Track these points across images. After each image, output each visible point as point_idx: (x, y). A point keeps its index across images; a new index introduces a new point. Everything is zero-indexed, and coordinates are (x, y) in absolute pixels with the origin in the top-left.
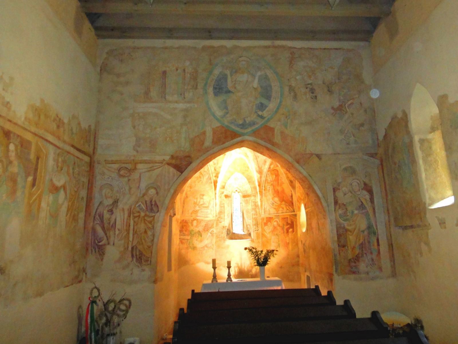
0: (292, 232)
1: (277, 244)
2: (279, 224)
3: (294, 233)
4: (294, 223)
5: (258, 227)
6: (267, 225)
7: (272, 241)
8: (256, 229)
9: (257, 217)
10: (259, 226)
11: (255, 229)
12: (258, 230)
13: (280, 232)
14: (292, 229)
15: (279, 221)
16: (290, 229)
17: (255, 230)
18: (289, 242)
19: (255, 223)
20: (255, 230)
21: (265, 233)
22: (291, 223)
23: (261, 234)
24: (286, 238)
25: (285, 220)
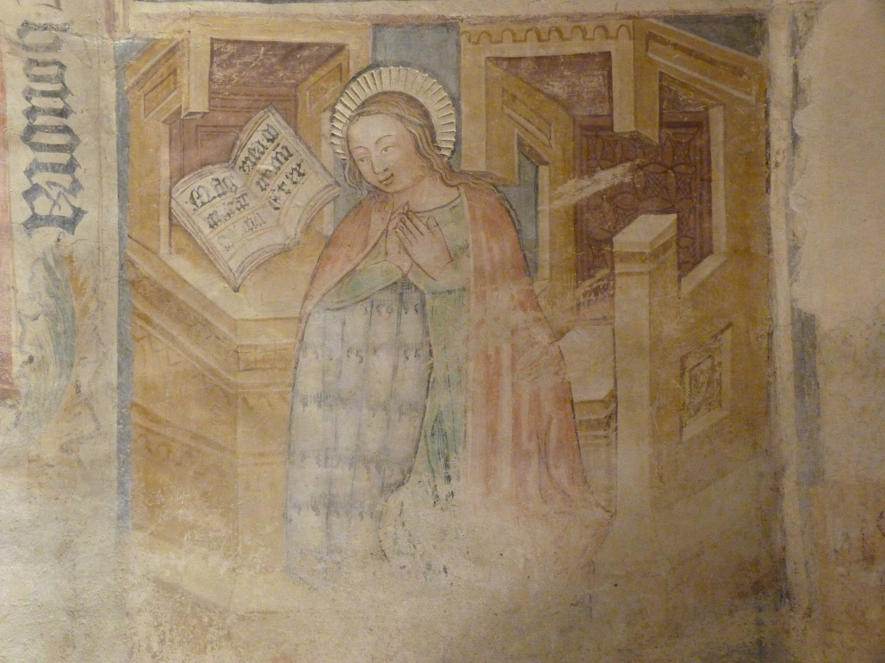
0: (671, 256)
1: (405, 428)
2: (445, 140)
3: (707, 267)
4: (717, 131)
5: (70, 167)
6: (227, 157)
7: (310, 384)
8: (42, 206)
9: (58, 19)
10: (84, 154)
11: (30, 194)
12: (69, 224)
13: (453, 258)
14: (673, 217)
15: (456, 102)
16: (627, 216)
17: (34, 222)
18: (613, 396)
19: (31, 112)
20: (34, 222)
21: (181, 265)
22: (652, 133)
23: (111, 289)
24: (560, 334)
25: (557, 88)
